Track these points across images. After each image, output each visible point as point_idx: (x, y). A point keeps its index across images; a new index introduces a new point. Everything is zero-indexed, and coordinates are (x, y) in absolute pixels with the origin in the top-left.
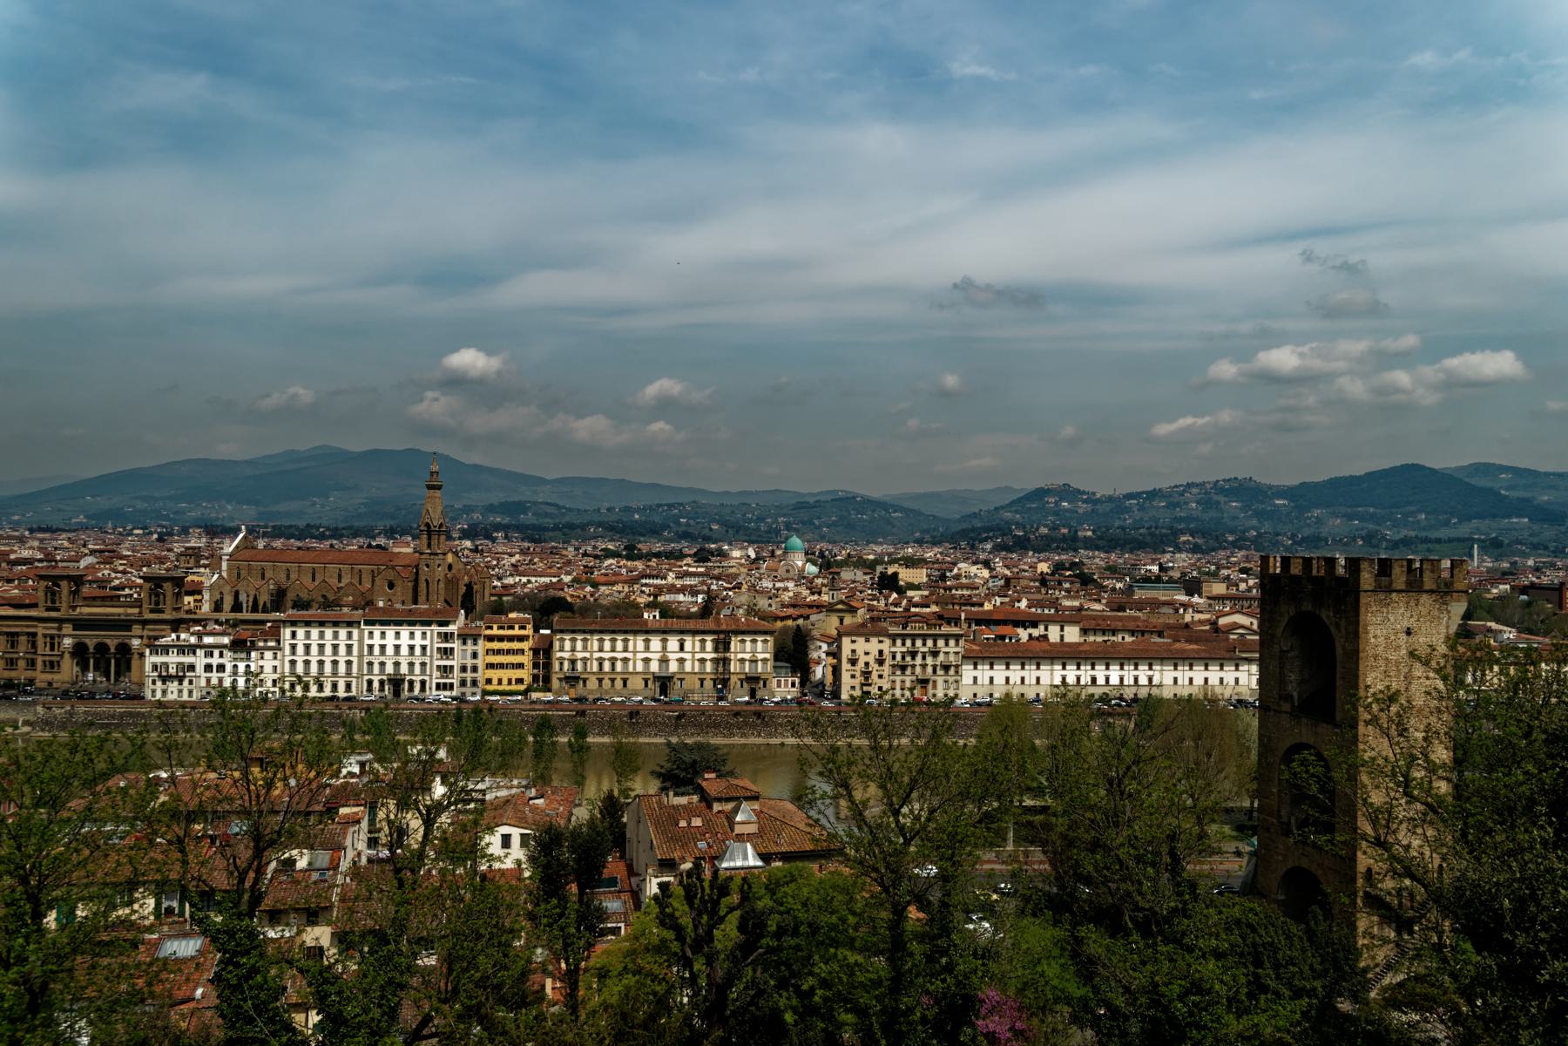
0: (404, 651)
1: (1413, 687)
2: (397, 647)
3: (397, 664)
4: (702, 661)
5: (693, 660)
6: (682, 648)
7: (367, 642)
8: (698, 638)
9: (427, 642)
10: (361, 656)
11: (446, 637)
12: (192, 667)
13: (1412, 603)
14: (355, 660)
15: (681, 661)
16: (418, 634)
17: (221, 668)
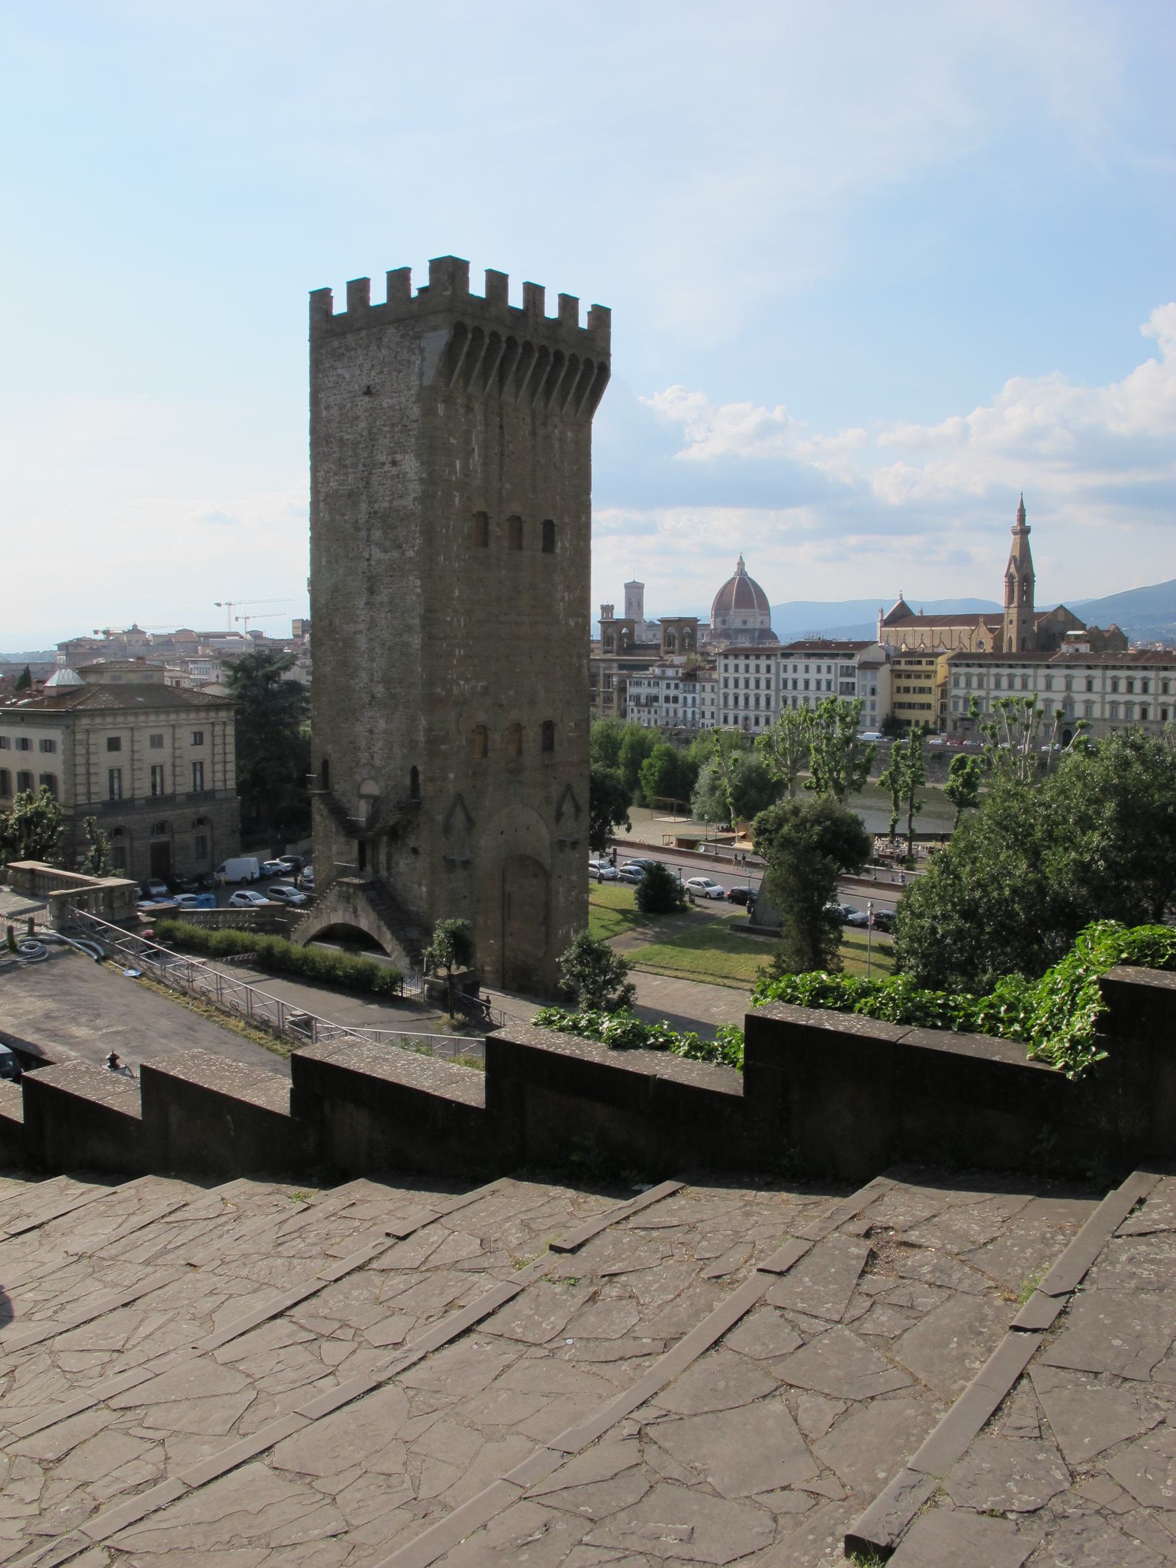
0: (813, 686)
1: (375, 480)
2: (807, 683)
3: (806, 699)
4: (1114, 704)
5: (1103, 703)
6: (1089, 688)
7: (783, 675)
8: (1110, 673)
9: (831, 677)
10: (777, 690)
11: (847, 672)
12: (656, 699)
13: (373, 347)
14: (772, 693)
15: (1089, 704)
16: (824, 669)
17: (676, 700)
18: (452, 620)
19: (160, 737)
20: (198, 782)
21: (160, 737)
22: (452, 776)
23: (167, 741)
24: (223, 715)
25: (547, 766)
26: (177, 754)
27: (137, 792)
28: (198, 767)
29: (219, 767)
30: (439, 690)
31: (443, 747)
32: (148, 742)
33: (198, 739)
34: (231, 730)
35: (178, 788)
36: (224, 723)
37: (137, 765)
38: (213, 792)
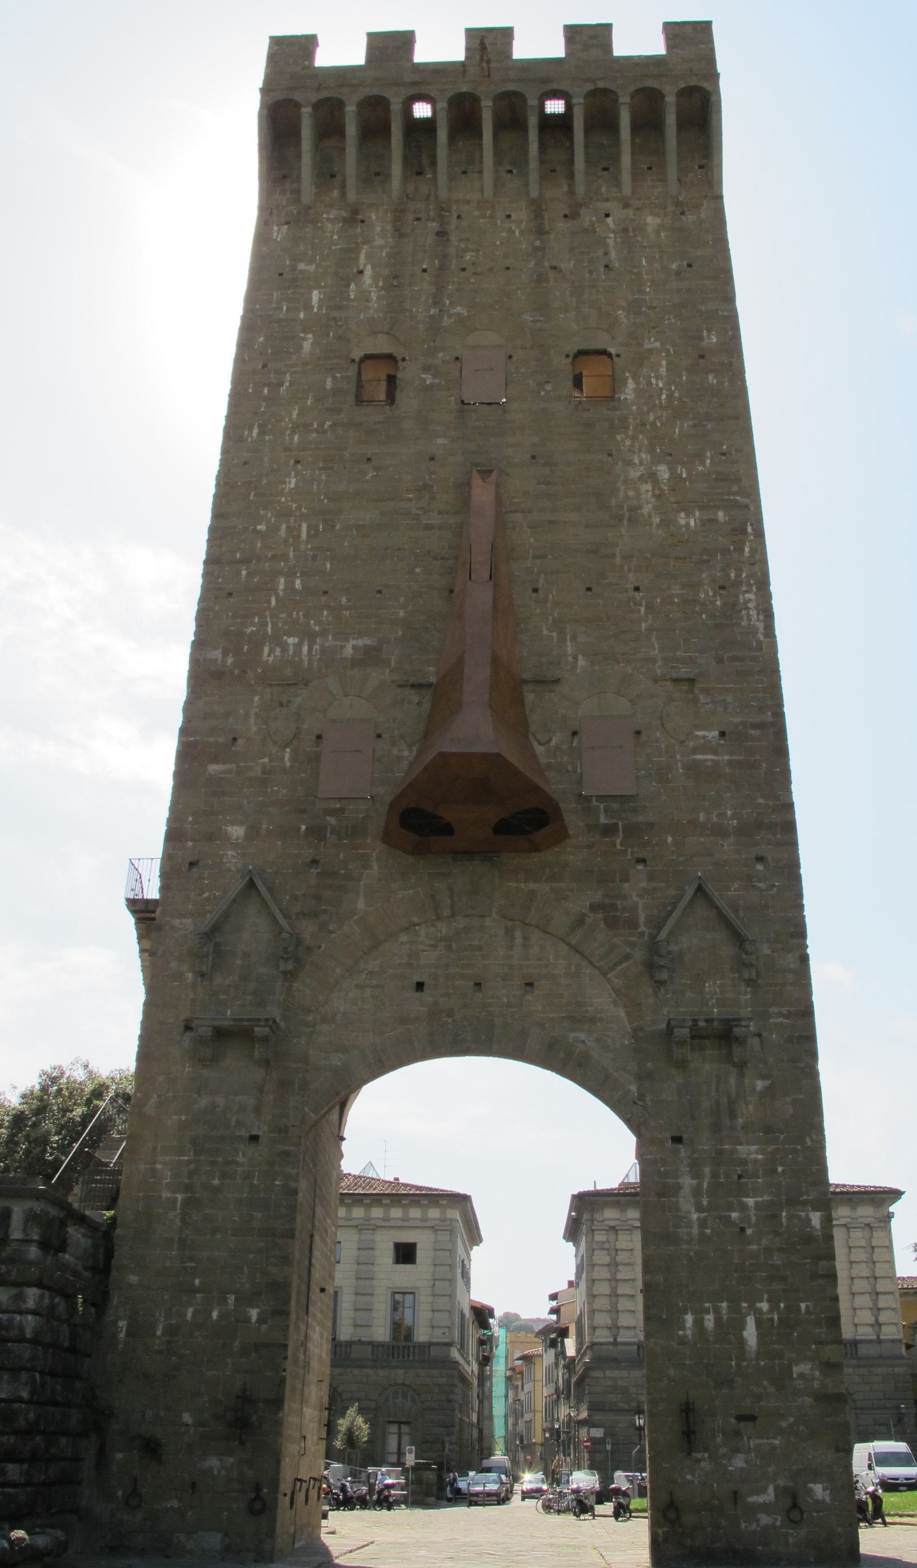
18: (274, 529)
22: (237, 832)
25: (609, 830)
30: (217, 654)
31: (213, 768)
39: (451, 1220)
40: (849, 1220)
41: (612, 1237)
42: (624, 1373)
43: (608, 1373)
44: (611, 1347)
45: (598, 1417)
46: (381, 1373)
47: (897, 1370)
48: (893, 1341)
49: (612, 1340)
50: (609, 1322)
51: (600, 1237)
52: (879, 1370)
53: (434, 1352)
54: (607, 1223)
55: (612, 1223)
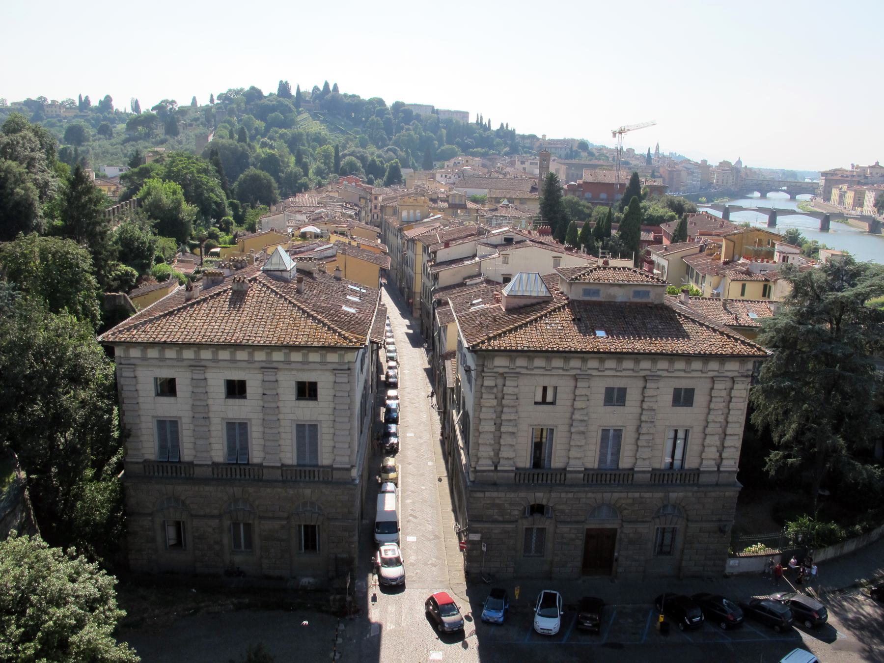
19: (622, 392)
20: (678, 455)
21: (622, 392)
23: (633, 397)
24: (732, 367)
26: (643, 418)
27: (572, 462)
28: (681, 434)
29: (713, 441)
32: (601, 397)
33: (683, 398)
34: (742, 391)
35: (639, 462)
36: (733, 379)
37: (578, 427)
38: (697, 472)
39: (349, 362)
40: (715, 374)
41: (500, 382)
42: (502, 495)
43: (488, 494)
44: (491, 474)
45: (476, 525)
46: (291, 492)
47: (727, 494)
48: (729, 472)
49: (493, 468)
50: (492, 454)
51: (488, 382)
52: (713, 494)
53: (336, 475)
54: (496, 370)
55: (501, 370)
